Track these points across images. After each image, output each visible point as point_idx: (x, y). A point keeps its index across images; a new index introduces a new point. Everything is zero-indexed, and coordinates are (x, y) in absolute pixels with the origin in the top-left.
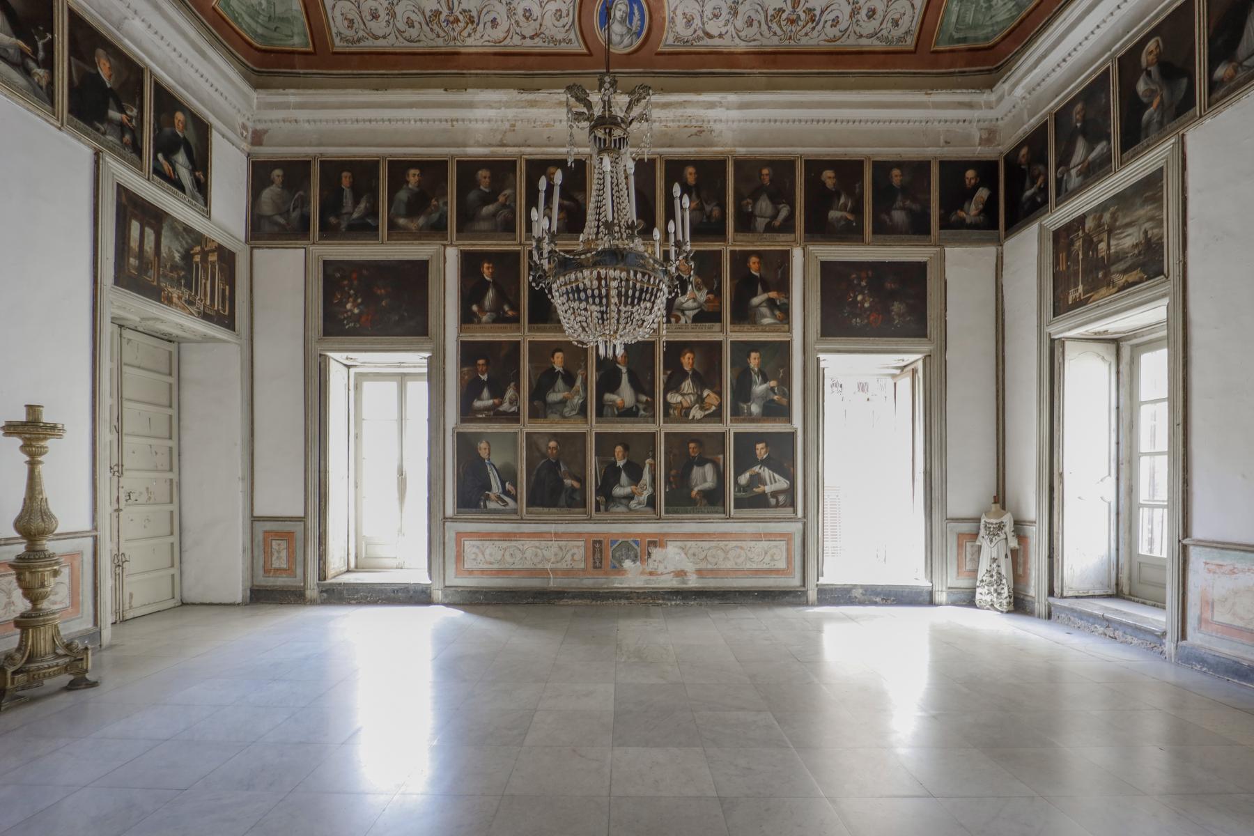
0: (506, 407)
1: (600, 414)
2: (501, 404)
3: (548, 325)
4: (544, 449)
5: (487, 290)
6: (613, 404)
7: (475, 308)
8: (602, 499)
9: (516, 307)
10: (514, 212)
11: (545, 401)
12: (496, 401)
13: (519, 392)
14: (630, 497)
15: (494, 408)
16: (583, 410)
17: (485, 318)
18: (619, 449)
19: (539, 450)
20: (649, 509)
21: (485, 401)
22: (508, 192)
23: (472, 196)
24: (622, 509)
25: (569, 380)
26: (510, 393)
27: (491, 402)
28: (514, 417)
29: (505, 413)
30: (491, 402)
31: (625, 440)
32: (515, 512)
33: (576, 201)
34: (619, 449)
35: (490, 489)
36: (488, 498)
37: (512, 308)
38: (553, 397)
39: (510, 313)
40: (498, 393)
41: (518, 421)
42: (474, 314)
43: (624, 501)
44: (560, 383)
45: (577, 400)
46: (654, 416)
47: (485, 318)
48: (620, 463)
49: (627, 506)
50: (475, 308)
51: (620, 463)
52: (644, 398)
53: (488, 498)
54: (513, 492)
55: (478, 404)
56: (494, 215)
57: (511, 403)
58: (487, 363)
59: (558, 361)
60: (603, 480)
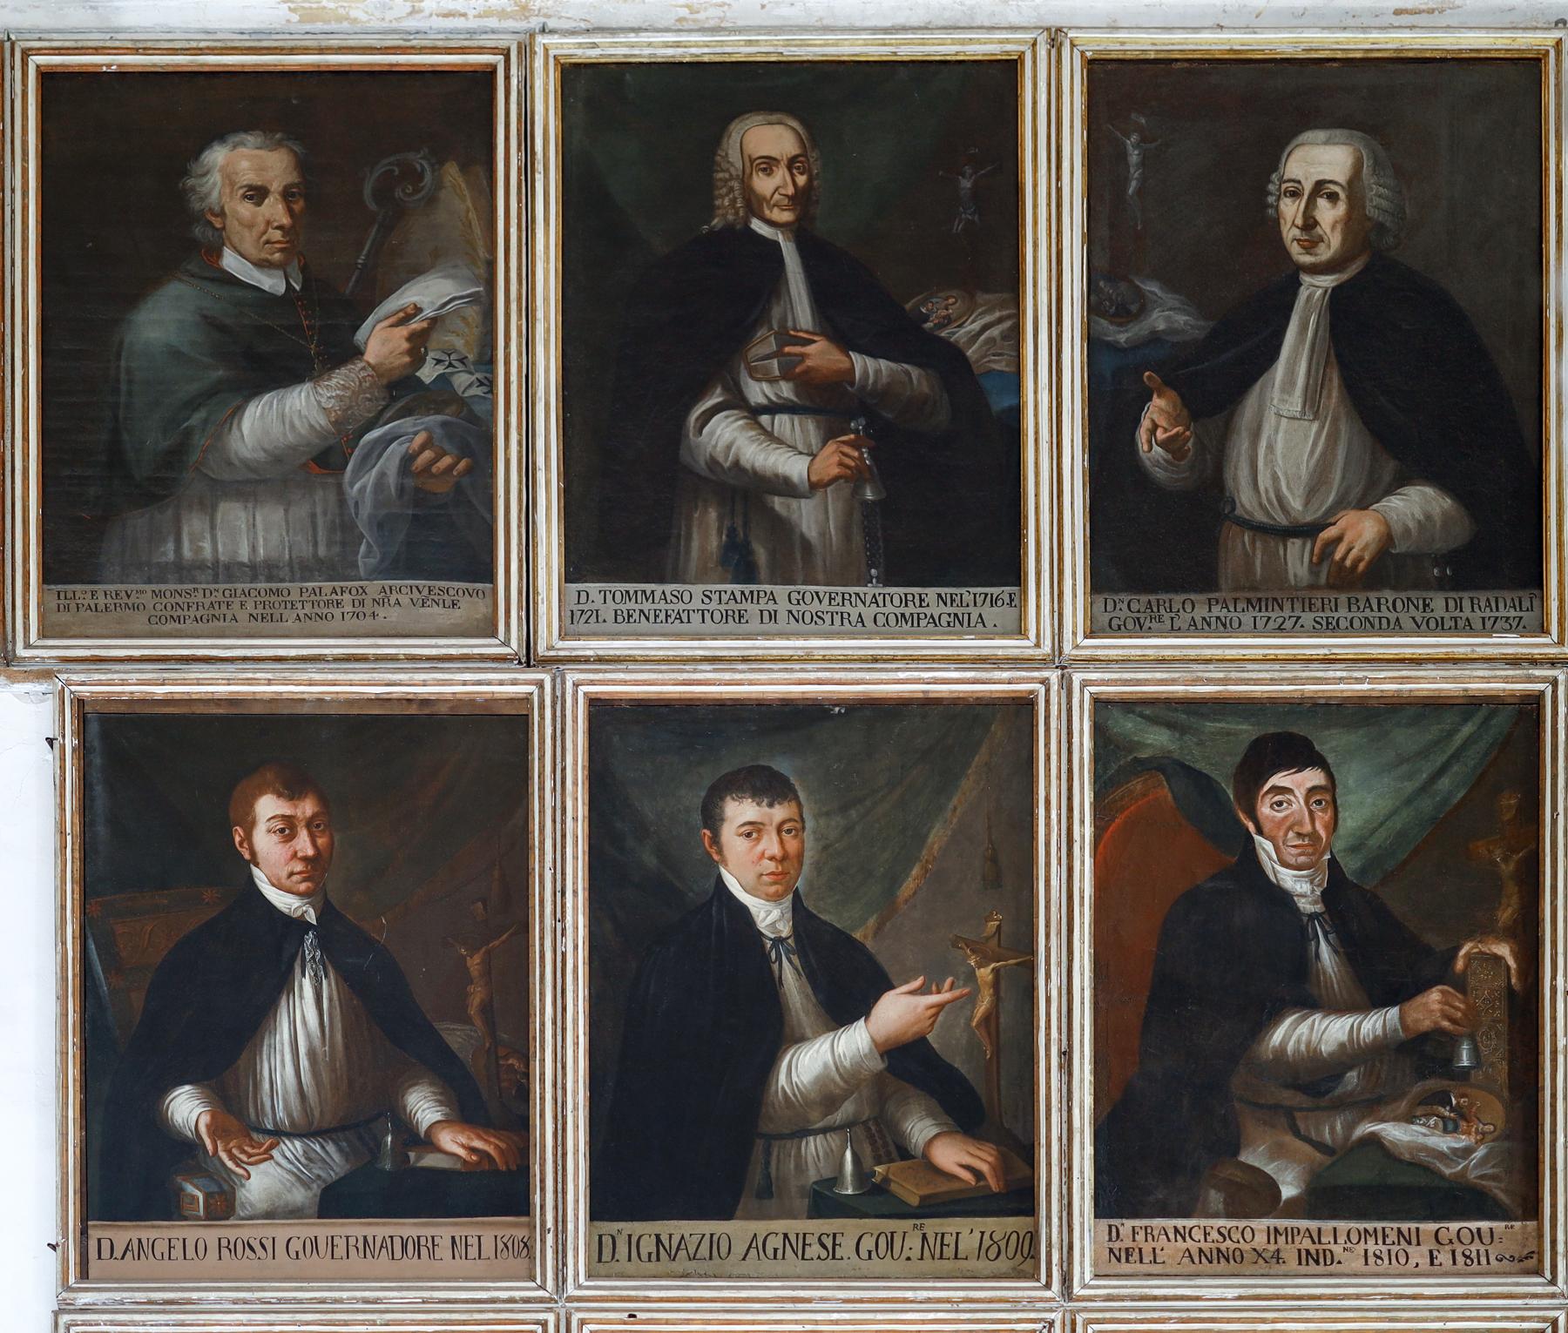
3: (737, 1230)
5: (282, 984)
7: (186, 1108)
9: (498, 1101)
10: (474, 439)
17: (264, 1181)
22: (429, 293)
23: (163, 321)
33: (948, 362)
37: (466, 1108)
39: (454, 1142)
42: (185, 1150)
47: (264, 1181)
50: (186, 1108)
56: (327, 457)
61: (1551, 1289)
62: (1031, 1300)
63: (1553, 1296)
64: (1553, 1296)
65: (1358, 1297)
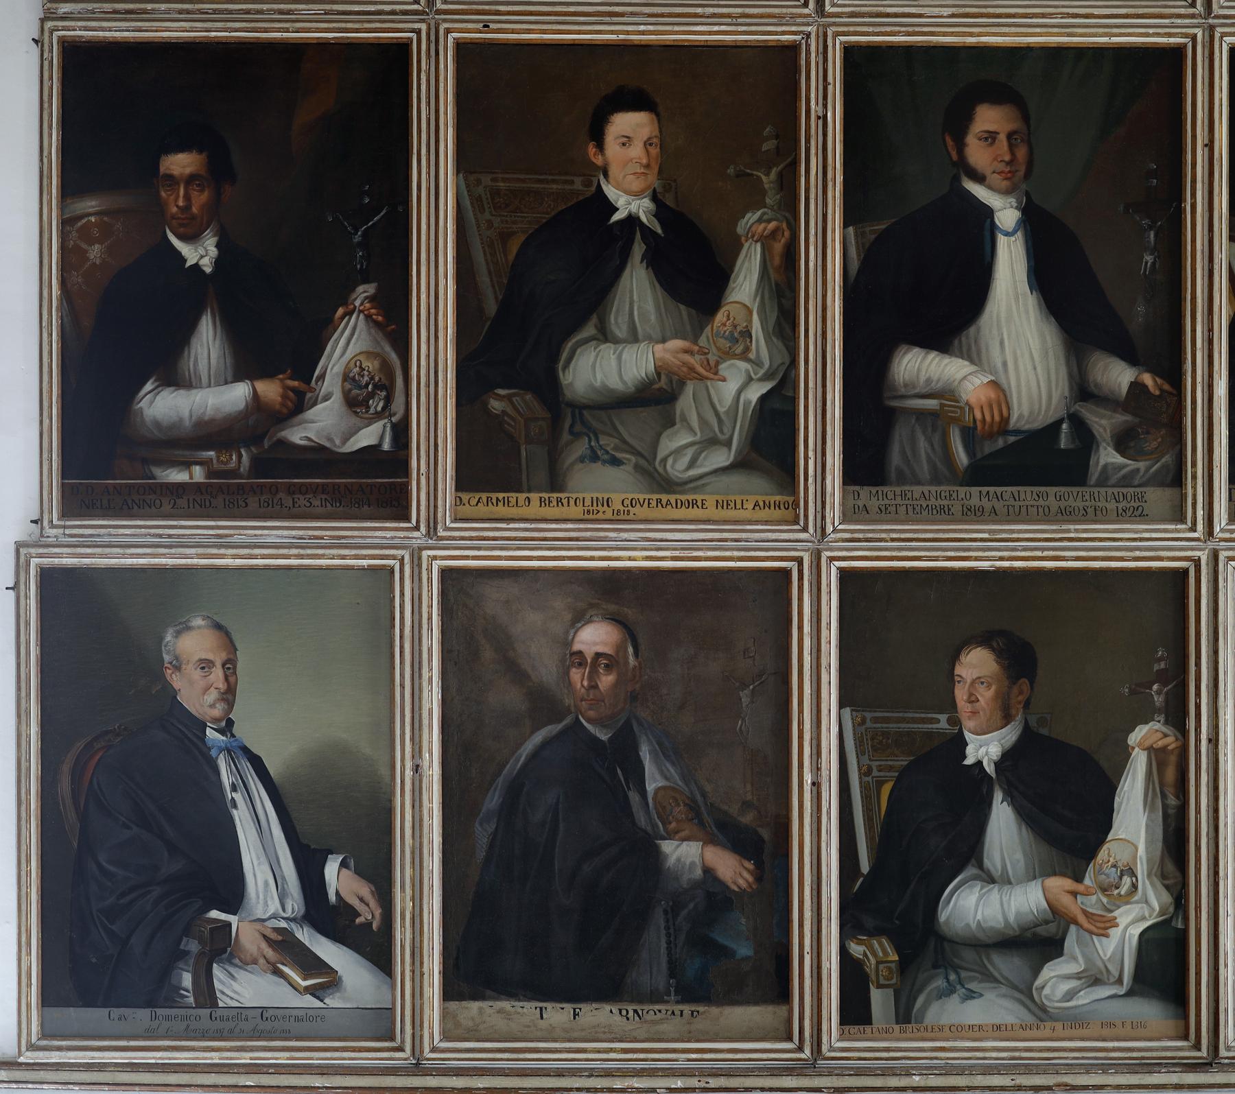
0: (323, 422)
1: (866, 464)
2: (298, 404)
4: (543, 664)
6: (943, 410)
8: (877, 952)
11: (548, 388)
12: (270, 390)
13: (401, 341)
14: (1039, 942)
15: (256, 426)
16: (770, 444)
18: (976, 665)
19: (515, 671)
20: (1150, 1011)
21: (206, 390)
24: (993, 1007)
25: (692, 269)
26: (348, 346)
27: (237, 395)
28: (373, 484)
29: (320, 459)
30: (237, 395)
31: (1012, 613)
32: (379, 1025)
34: (976, 665)
35: (234, 898)
36: (220, 946)
38: (600, 368)
40: (279, 344)
41: (394, 504)
43: (1007, 965)
44: (637, 290)
45: (737, 387)
46: (1176, 478)
48: (985, 749)
49: (1025, 992)
51: (985, 749)
52: (1118, 375)
53: (220, 946)
54: (369, 913)
55: (162, 406)
57: (354, 403)
58: (219, 172)
59: (628, 164)
60: (884, 846)
61: (1191, 11)
62: (793, 16)
63: (1193, 16)
64: (1193, 16)
65: (1043, 16)
